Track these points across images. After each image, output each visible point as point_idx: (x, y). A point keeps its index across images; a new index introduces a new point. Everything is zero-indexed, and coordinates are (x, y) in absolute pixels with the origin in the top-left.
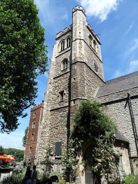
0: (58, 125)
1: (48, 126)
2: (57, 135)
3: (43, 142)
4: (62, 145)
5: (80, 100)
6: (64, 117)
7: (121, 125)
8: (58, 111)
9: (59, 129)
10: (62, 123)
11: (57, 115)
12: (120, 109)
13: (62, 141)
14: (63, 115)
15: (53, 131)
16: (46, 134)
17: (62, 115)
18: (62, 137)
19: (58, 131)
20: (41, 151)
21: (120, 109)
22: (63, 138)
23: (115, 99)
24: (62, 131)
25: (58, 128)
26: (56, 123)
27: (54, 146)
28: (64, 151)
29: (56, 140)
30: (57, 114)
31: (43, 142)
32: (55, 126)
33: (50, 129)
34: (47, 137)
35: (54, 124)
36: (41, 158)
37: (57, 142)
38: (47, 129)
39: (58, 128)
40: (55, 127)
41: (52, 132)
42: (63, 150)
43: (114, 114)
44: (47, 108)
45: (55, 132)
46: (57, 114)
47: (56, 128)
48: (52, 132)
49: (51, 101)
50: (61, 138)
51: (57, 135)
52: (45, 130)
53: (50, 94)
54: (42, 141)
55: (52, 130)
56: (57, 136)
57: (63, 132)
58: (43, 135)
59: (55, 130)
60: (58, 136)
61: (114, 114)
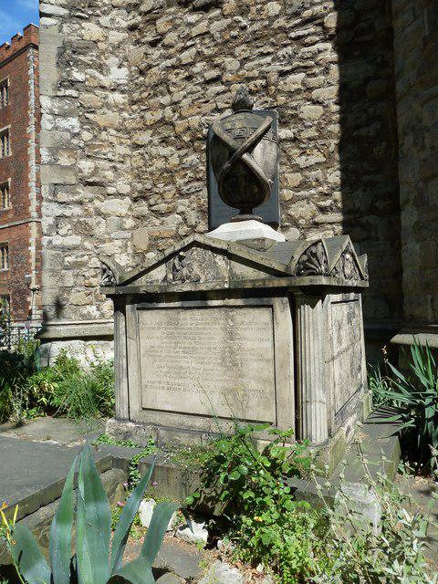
2: (209, 59)
3: (87, 136)
13: (281, 99)
15: (169, 39)
16: (101, 68)
18: (277, 67)
19: (217, 26)
20: (77, 210)
22: (283, 74)
27: (193, 158)
28: (304, 185)
29: (207, 108)
31: (87, 136)
34: (117, 98)
36: (83, 264)
38: (104, 20)
41: (153, 44)
42: (295, 178)
48: (153, 44)
50: (263, 76)
51: (209, 59)
52: (91, 30)
54: (73, 122)
55: (162, 25)
56: (213, 73)
57: (281, 22)
58: (77, 75)
59: (193, 18)
60: (231, 63)
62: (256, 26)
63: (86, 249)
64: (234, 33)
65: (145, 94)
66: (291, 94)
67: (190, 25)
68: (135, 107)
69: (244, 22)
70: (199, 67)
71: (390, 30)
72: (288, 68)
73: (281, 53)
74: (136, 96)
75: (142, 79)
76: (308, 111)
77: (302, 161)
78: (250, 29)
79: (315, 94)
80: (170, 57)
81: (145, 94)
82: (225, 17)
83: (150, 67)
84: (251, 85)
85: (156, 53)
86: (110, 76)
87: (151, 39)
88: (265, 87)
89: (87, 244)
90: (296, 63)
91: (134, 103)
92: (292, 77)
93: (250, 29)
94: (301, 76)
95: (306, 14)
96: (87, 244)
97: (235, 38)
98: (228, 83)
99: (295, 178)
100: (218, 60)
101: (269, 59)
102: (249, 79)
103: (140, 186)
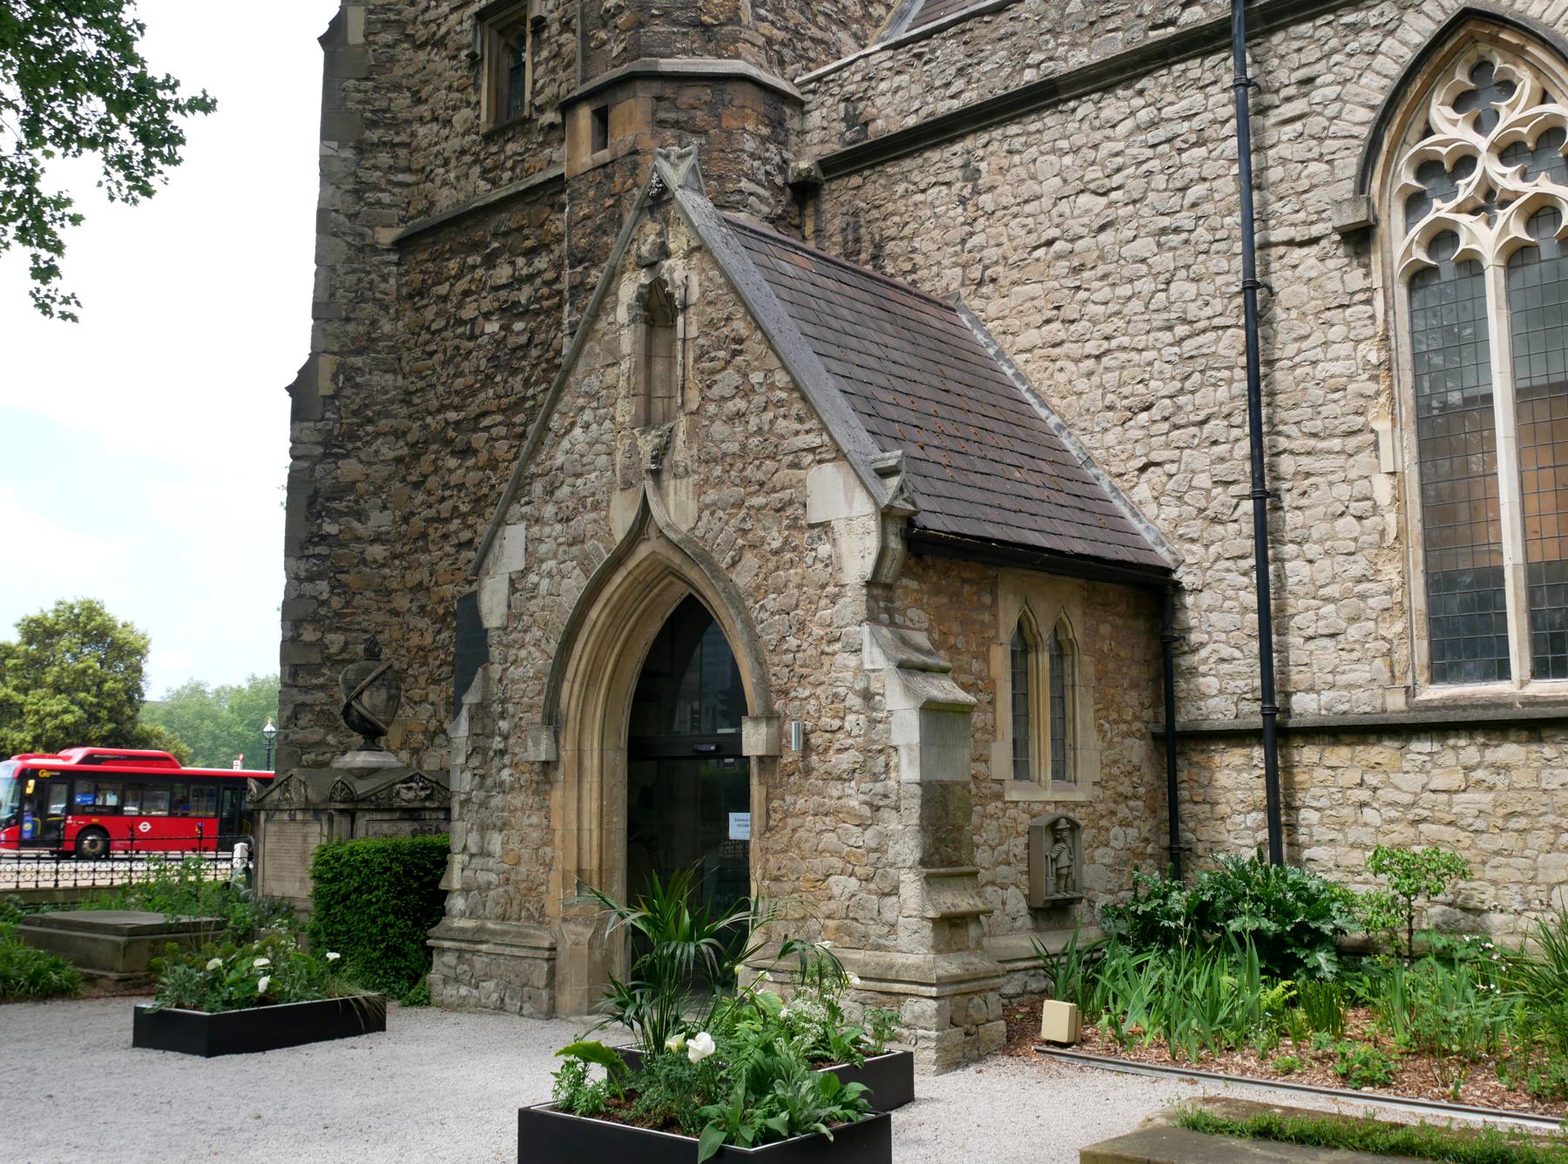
0: (473, 409)
1: (384, 424)
2: (464, 516)
3: (336, 602)
5: (669, 91)
6: (537, 313)
7: (1111, 379)
8: (474, 247)
9: (483, 456)
10: (517, 382)
11: (466, 293)
12: (1117, 180)
14: (524, 295)
15: (433, 482)
16: (361, 516)
17: (513, 296)
19: (474, 476)
20: (320, 696)
21: (1117, 180)
23: (1081, 58)
25: (479, 439)
26: (459, 383)
30: (462, 285)
31: (336, 602)
32: (452, 416)
33: (399, 460)
34: (377, 551)
35: (435, 404)
39: (479, 439)
40: (451, 434)
41: (417, 486)
43: (1050, 243)
44: (352, 217)
45: (446, 486)
46: (462, 285)
47: (460, 441)
49: (396, 124)
52: (350, 469)
53: (387, 37)
54: (323, 586)
55: (425, 465)
56: (465, 535)
58: (330, 528)
59: (452, 463)
61: (1050, 243)
63: (328, 745)
64: (485, 490)
65: (407, 548)
67: (450, 471)
68: (397, 562)
74: (398, 549)
75: (404, 527)
81: (407, 548)
82: (479, 469)
83: (412, 514)
85: (420, 497)
86: (370, 524)
87: (414, 479)
89: (331, 739)
91: (395, 556)
96: (331, 739)
97: (486, 496)
100: (471, 520)
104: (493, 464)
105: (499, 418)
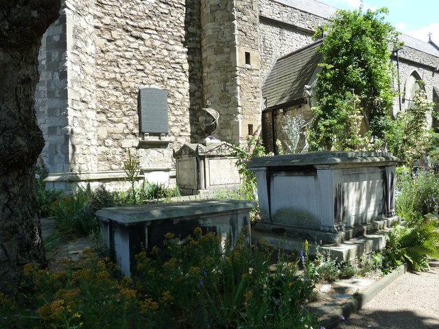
2: (139, 61)
4: (169, 100)
10: (164, 24)
13: (168, 88)
22: (168, 78)
24: (166, 53)
27: (130, 100)
28: (176, 121)
29: (139, 81)
32: (131, 23)
37: (142, 87)
42: (173, 118)
47: (135, 33)
48: (109, 41)
51: (139, 61)
56: (141, 67)
62: (159, 56)
64: (150, 55)
66: (172, 87)
68: (98, 67)
69: (154, 52)
70: (134, 62)
71: (202, 77)
72: (170, 77)
73: (168, 70)
74: (99, 62)
76: (177, 95)
77: (175, 112)
78: (156, 56)
79: (180, 90)
80: (119, 51)
81: (105, 63)
84: (157, 78)
85: (111, 46)
88: (163, 81)
90: (173, 77)
91: (98, 64)
92: (171, 81)
93: (156, 56)
94: (175, 82)
95: (177, 60)
98: (147, 74)
99: (173, 118)
100: (142, 63)
101: (163, 71)
102: (156, 76)
103: (101, 107)
104: (154, 48)
105: (155, 32)
